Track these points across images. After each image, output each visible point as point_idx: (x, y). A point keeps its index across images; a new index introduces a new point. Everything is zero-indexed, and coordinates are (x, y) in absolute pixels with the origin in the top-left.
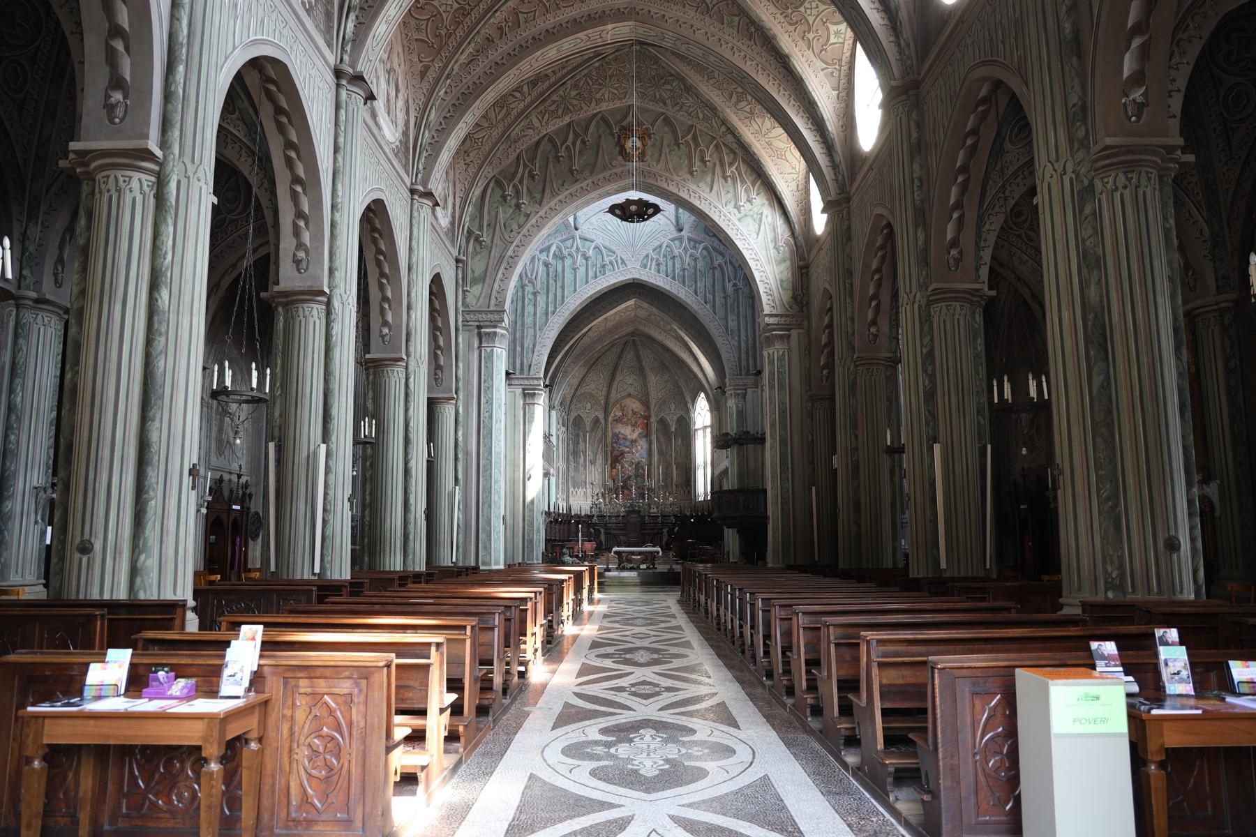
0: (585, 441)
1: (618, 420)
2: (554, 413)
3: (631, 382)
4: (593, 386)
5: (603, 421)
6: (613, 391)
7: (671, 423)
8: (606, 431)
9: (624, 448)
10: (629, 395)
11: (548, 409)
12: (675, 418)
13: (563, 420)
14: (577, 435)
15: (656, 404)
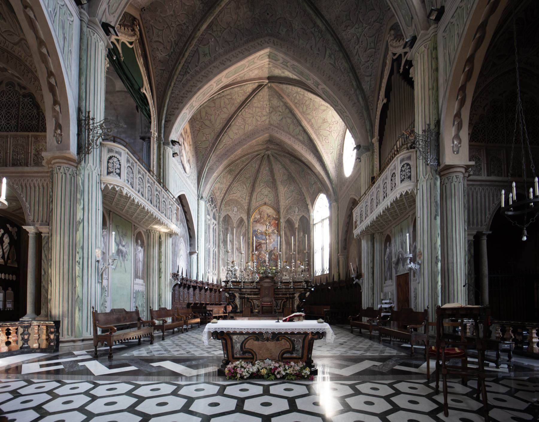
0: (233, 234)
1: (257, 221)
2: (202, 203)
3: (266, 193)
4: (238, 195)
5: (246, 221)
6: (254, 201)
7: (295, 222)
8: (248, 228)
9: (261, 241)
10: (265, 204)
11: (197, 198)
12: (298, 218)
13: (214, 214)
14: (227, 229)
15: (284, 209)
